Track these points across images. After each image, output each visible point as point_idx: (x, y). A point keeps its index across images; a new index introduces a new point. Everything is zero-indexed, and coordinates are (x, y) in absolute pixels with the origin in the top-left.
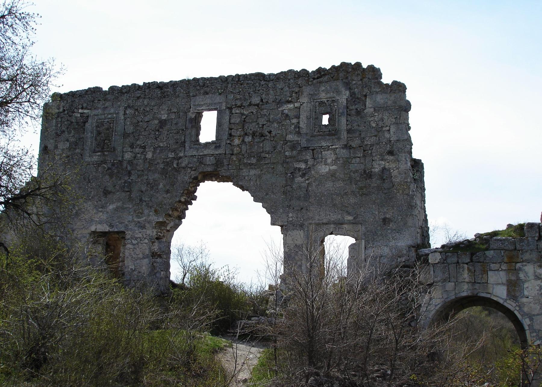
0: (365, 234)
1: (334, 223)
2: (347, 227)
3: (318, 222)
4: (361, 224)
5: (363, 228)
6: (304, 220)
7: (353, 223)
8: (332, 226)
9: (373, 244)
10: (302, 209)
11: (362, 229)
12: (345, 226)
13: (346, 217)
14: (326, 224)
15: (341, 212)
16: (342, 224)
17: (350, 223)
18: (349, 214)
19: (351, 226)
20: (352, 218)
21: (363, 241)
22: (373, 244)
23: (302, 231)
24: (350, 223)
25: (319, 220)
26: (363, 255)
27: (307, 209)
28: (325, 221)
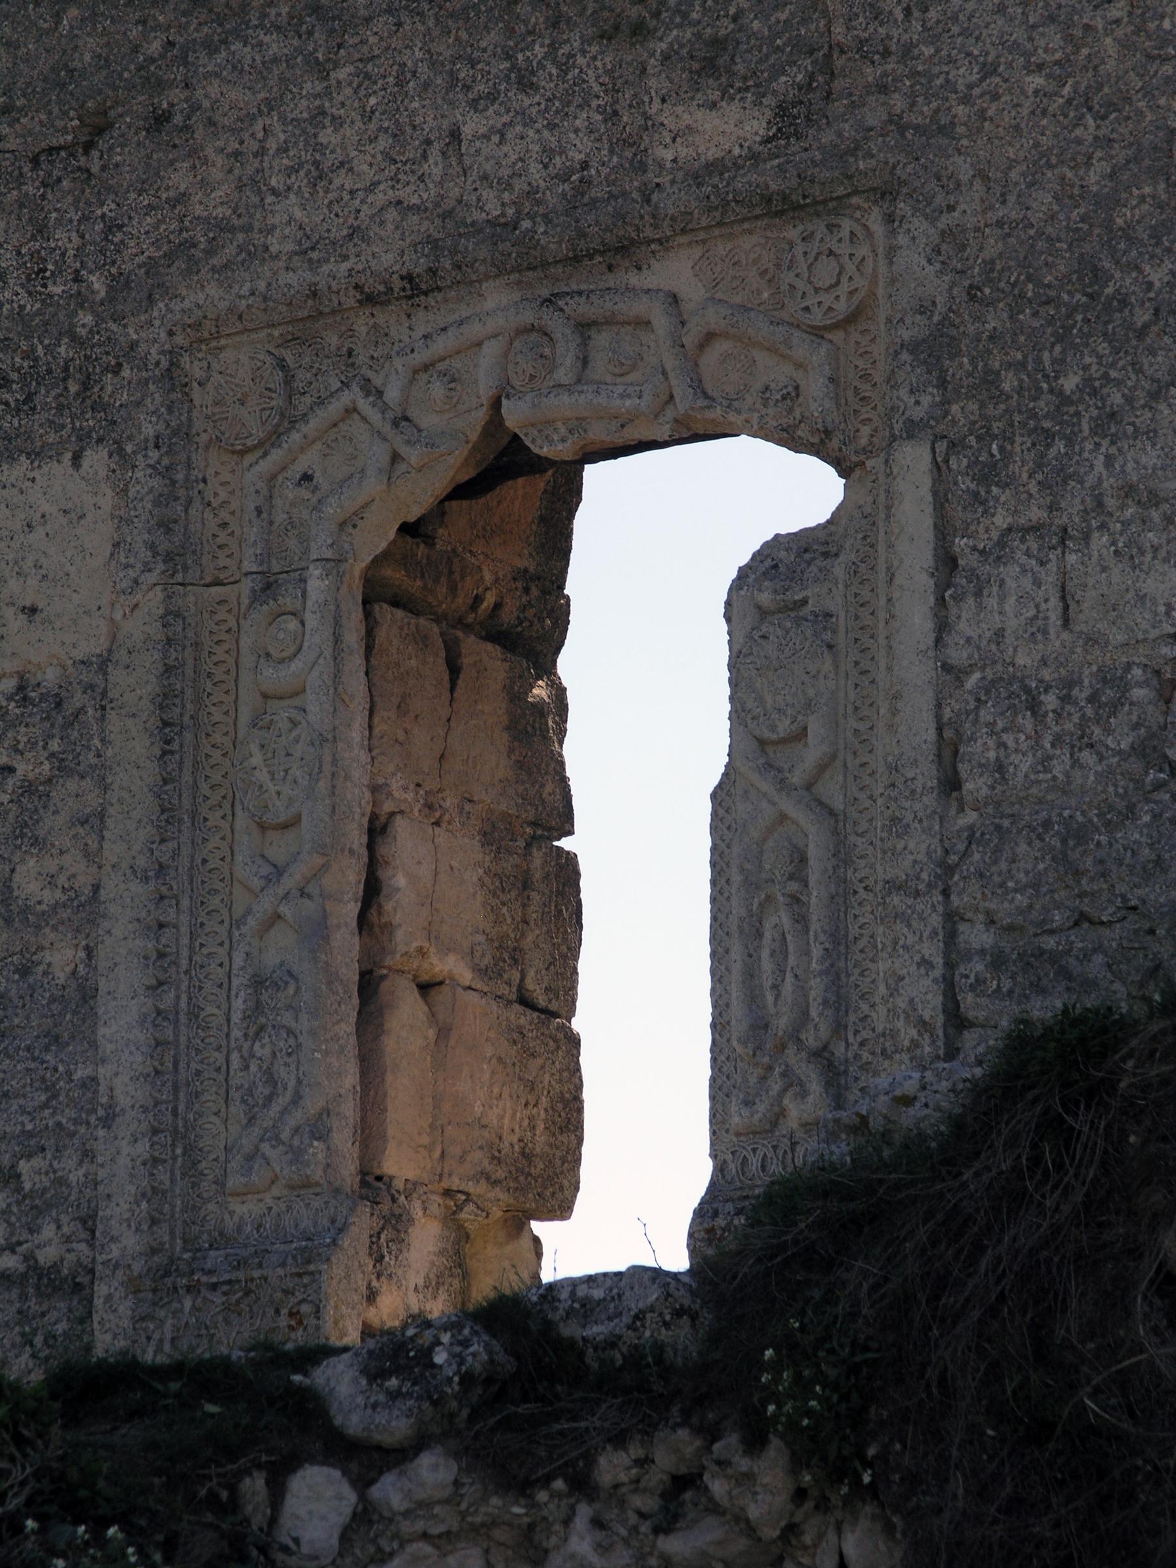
0: (933, 349)
1: (512, 250)
2: (692, 291)
3: (295, 280)
4: (885, 193)
5: (912, 259)
6: (120, 284)
7: (781, 207)
8: (498, 305)
9: (1057, 480)
10: (97, 129)
11: (899, 266)
12: (677, 271)
13: (672, 116)
14: (416, 289)
15: (594, 65)
16: (624, 251)
17: (734, 201)
18: (712, 66)
19: (751, 245)
20: (756, 126)
21: (915, 458)
22: (1057, 480)
23: (96, 459)
24: (734, 201)
25: (309, 248)
26: (914, 670)
27: (159, 120)
28: (387, 256)
